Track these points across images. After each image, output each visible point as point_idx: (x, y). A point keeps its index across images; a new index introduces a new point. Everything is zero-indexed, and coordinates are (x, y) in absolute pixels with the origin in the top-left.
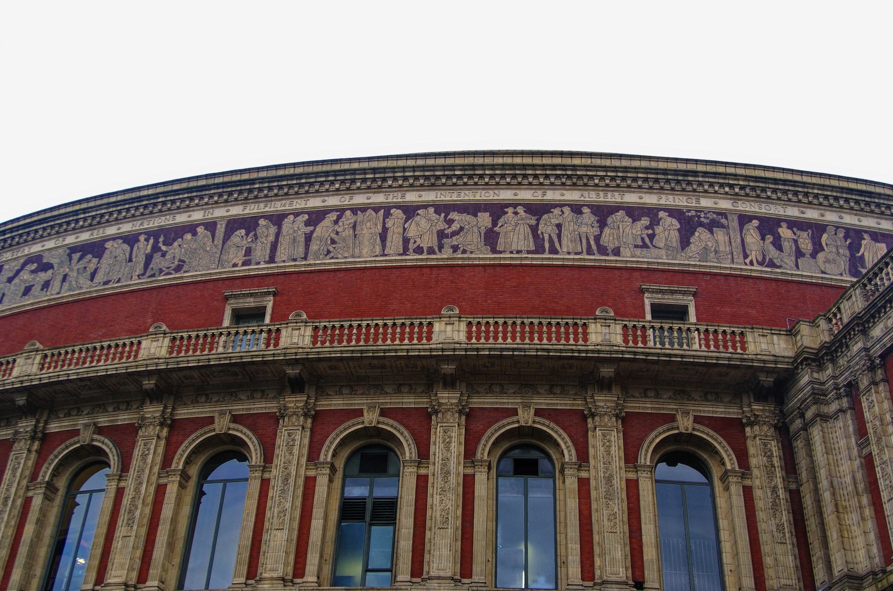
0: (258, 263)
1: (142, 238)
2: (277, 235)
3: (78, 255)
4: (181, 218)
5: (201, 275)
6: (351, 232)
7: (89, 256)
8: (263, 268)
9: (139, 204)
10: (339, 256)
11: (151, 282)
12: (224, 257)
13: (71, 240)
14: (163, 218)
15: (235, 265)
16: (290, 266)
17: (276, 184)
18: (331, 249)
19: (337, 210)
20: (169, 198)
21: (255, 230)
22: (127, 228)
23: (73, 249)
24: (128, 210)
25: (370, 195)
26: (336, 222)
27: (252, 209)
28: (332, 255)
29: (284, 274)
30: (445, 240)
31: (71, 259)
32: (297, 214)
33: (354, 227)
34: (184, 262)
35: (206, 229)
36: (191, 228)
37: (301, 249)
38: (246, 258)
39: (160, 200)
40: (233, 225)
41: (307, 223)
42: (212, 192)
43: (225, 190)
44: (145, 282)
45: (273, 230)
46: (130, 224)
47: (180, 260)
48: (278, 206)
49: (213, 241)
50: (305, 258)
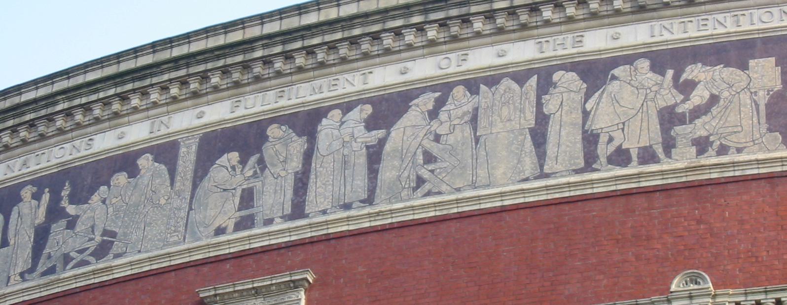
0: (269, 222)
1: (27, 193)
2: (308, 156)
4: (105, 142)
5: (150, 259)
6: (468, 130)
8: (283, 232)
9: (17, 121)
10: (444, 188)
11: (46, 285)
12: (196, 216)
14: (67, 146)
15: (220, 231)
16: (340, 222)
17: (298, 45)
18: (426, 175)
19: (433, 89)
20: (77, 102)
21: (259, 150)
25: (505, 47)
26: (433, 114)
27: (254, 104)
28: (427, 187)
29: (327, 239)
30: (678, 129)
32: (347, 107)
33: (474, 120)
34: (113, 234)
35: (156, 160)
36: (126, 162)
37: (360, 182)
38: (244, 213)
39: (59, 108)
40: (215, 143)
41: (371, 124)
42: (166, 77)
43: (192, 70)
45: (299, 145)
47: (105, 233)
48: (304, 94)
49: (172, 183)
50: (369, 201)
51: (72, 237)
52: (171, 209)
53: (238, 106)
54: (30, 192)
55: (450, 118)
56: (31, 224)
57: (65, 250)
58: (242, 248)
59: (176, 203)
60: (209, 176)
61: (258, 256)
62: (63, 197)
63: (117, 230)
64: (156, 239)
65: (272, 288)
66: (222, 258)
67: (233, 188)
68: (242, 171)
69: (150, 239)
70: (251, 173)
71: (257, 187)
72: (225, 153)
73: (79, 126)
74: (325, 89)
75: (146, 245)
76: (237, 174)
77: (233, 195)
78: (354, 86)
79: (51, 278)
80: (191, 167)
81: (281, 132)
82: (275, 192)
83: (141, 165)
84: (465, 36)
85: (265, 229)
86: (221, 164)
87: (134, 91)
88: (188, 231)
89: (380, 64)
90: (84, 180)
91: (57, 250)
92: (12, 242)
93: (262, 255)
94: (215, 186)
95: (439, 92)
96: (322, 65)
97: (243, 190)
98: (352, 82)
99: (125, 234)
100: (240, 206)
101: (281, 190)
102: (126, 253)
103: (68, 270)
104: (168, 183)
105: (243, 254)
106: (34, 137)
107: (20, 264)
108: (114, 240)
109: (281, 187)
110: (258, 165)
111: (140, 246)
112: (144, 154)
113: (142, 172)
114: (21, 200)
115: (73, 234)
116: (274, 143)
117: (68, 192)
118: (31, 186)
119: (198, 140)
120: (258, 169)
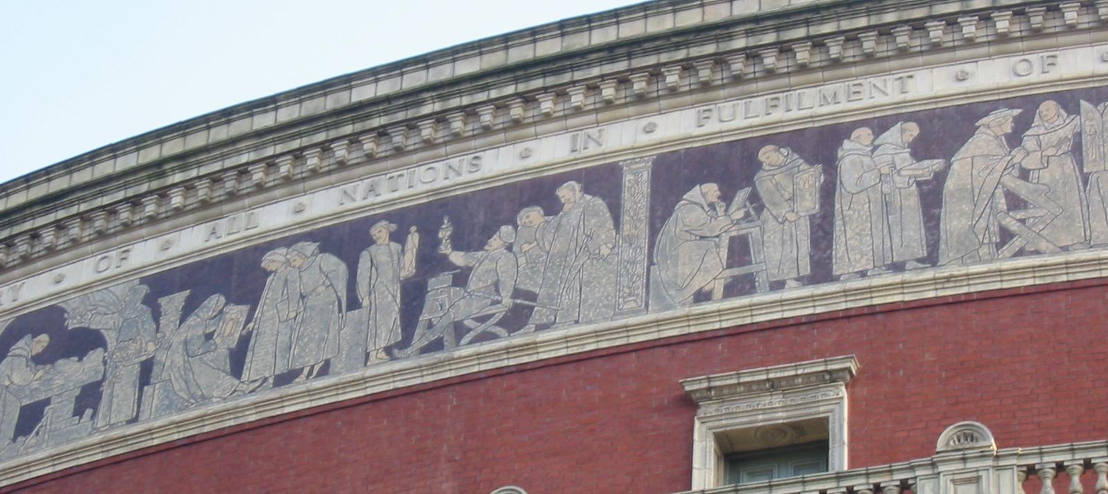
0: (778, 285)
1: (381, 232)
2: (828, 193)
3: (180, 298)
4: (500, 162)
5: (597, 334)
6: (1069, 164)
7: (216, 301)
8: (799, 300)
9: (359, 127)
10: (1043, 245)
11: (432, 366)
12: (661, 274)
13: (146, 253)
15: (702, 296)
16: (888, 290)
17: (800, 32)
18: (1014, 226)
19: (1009, 103)
20: (454, 102)
21: (749, 181)
22: (323, 204)
23: (159, 284)
24: (325, 147)
26: (1014, 139)
27: (732, 117)
28: (1017, 243)
29: (871, 312)
31: (156, 315)
32: (880, 125)
33: (1077, 150)
34: (532, 297)
35: (586, 190)
36: (541, 191)
37: (913, 235)
38: (736, 271)
39: (427, 109)
40: (677, 172)
41: (920, 150)
42: (596, 71)
44: (411, 370)
45: (810, 177)
46: (335, 193)
47: (517, 293)
48: (810, 104)
50: (931, 259)
51: (464, 298)
52: (619, 263)
54: (386, 230)
55: (1040, 147)
56: (393, 277)
57: (454, 316)
58: (740, 322)
59: (628, 253)
60: (674, 216)
61: (767, 333)
62: (442, 240)
63: (537, 290)
64: (601, 305)
66: (709, 335)
67: (714, 235)
68: (726, 210)
69: (592, 305)
70: (740, 214)
71: (754, 235)
72: (695, 185)
73: (457, 137)
74: (842, 97)
75: (587, 313)
76: (719, 214)
77: (717, 246)
78: (887, 95)
79: (437, 356)
80: (644, 204)
81: (782, 158)
82: (783, 243)
83: (563, 197)
84: (1052, 30)
86: (693, 200)
87: (545, 90)
88: (650, 296)
89: (924, 65)
91: (441, 317)
92: (365, 302)
93: (772, 332)
94: (686, 231)
95: (1019, 108)
96: (836, 63)
97: (732, 239)
98: (883, 89)
99: (550, 297)
100: (730, 261)
101: (792, 241)
102: (555, 323)
103: (463, 345)
104: (610, 224)
105: (742, 330)
107: (383, 335)
108: (534, 304)
109: (791, 236)
110: (751, 203)
111: (577, 315)
112: (566, 182)
113: (566, 208)
115: (466, 295)
116: (771, 173)
117: (449, 233)
118: (387, 222)
119: (650, 163)
120: (751, 210)
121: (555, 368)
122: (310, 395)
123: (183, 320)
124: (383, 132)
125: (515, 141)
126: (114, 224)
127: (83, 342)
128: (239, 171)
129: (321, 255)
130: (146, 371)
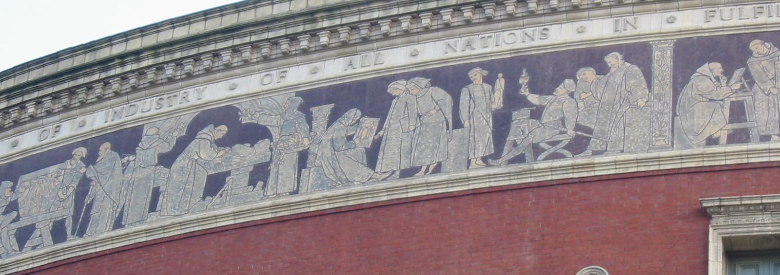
1: (476, 75)
3: (327, 109)
4: (562, 34)
5: (637, 161)
7: (354, 114)
11: (518, 173)
12: (682, 123)
13: (300, 75)
14: (518, 32)
15: (712, 141)
21: (743, 64)
22: (433, 52)
23: (311, 98)
31: (309, 120)
34: (590, 131)
35: (626, 59)
36: (593, 57)
38: (736, 126)
40: (692, 52)
44: (500, 174)
46: (441, 44)
47: (578, 127)
49: (650, 86)
51: (539, 127)
52: (652, 113)
53: (713, 16)
54: (480, 75)
56: (487, 108)
57: (532, 139)
58: (739, 161)
59: (658, 107)
60: (690, 83)
61: (758, 171)
62: (522, 85)
63: (592, 126)
64: (639, 141)
65: (771, 207)
66: (717, 169)
67: (720, 99)
68: (728, 83)
69: (633, 141)
70: (737, 86)
71: (748, 101)
72: (706, 62)
75: (629, 146)
76: (723, 85)
77: (722, 107)
79: (521, 166)
80: (668, 73)
81: (766, 50)
82: (769, 109)
83: (610, 62)
85: (742, 146)
86: (703, 73)
88: (675, 137)
90: (552, 70)
91: (523, 139)
92: (467, 124)
93: (762, 170)
94: (699, 95)
97: (732, 103)
99: (603, 132)
100: (731, 119)
101: (775, 107)
102: (606, 150)
103: (540, 161)
104: (644, 85)
105: (740, 167)
106: (458, 22)
107: (481, 148)
108: (591, 136)
109: (774, 104)
110: (745, 80)
111: (622, 146)
112: (611, 52)
113: (612, 70)
114: (470, 82)
115: (540, 125)
116: (759, 59)
117: (526, 81)
118: (481, 69)
119: (672, 45)
120: (745, 83)
121: (606, 182)
122: (427, 186)
123: (329, 125)
124: (478, 5)
125: (574, 20)
126: (276, 52)
127: (255, 134)
128: (371, 23)
129: (432, 88)
130: (303, 159)
